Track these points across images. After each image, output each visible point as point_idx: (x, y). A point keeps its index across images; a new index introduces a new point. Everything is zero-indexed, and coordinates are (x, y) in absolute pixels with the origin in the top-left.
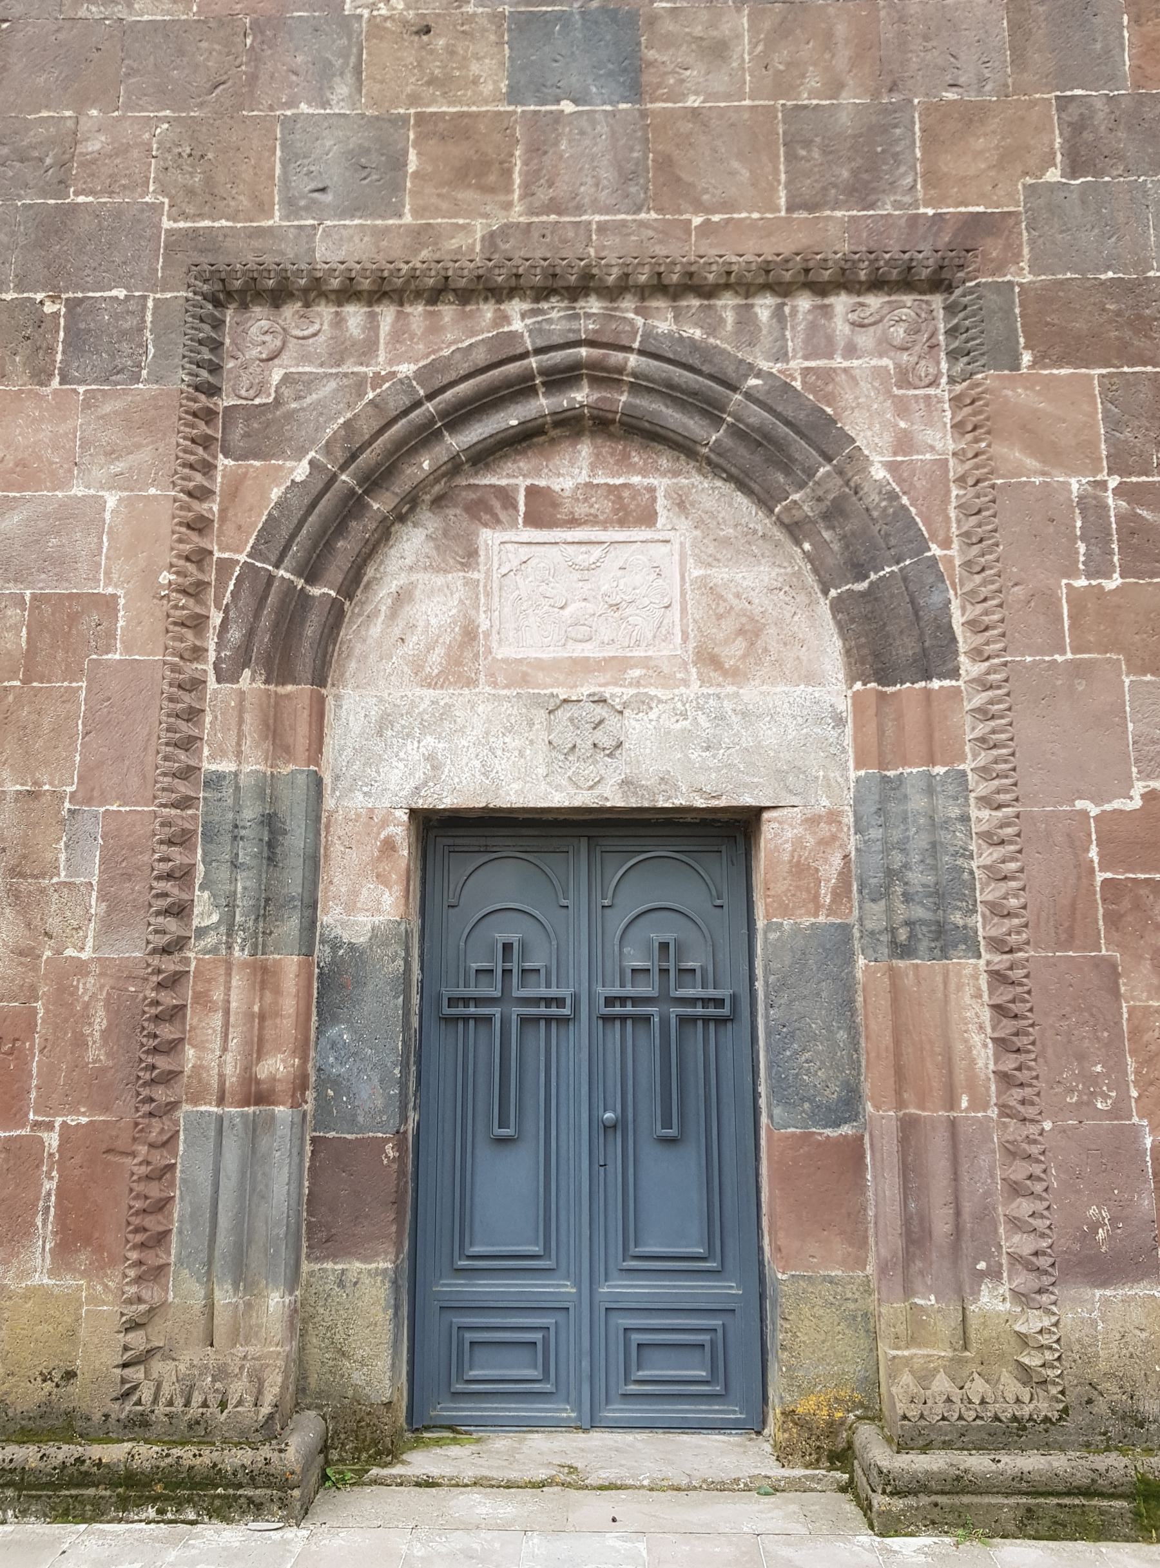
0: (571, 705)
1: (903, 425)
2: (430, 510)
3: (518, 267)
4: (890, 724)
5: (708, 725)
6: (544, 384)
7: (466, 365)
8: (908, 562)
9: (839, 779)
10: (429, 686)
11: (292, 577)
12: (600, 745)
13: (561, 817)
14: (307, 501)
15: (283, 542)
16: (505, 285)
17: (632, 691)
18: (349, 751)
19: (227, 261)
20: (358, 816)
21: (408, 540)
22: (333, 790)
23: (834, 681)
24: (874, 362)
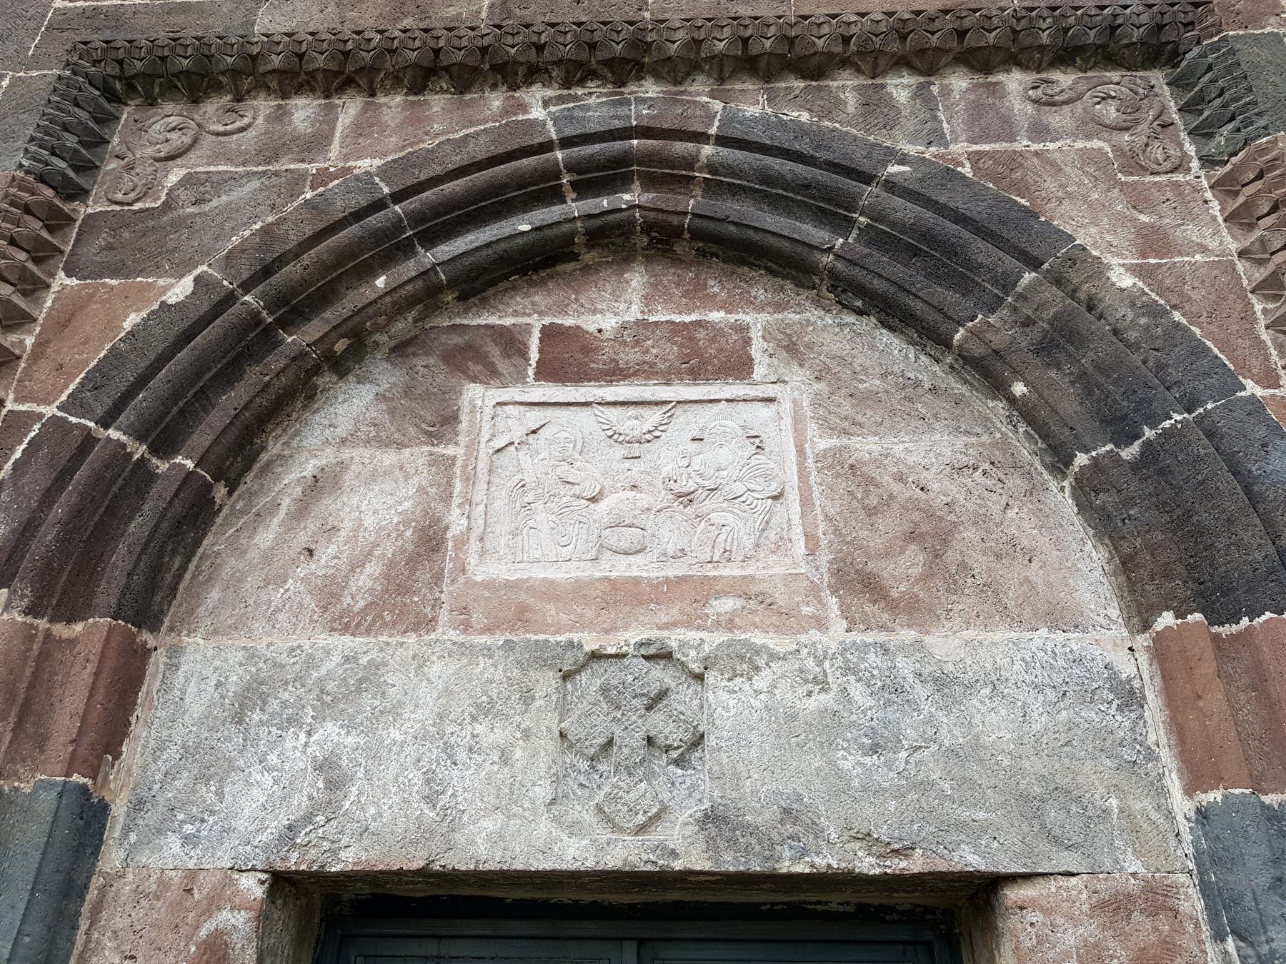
0: (605, 664)
1: (1144, 218)
2: (387, 360)
3: (540, 34)
4: (1242, 697)
5: (869, 702)
6: (574, 185)
7: (458, 158)
8: (1210, 406)
9: (1154, 815)
10: (345, 629)
11: (124, 438)
12: (661, 740)
13: (587, 898)
14: (177, 329)
15: (123, 386)
16: (522, 59)
17: (720, 637)
18: (173, 752)
19: (129, 37)
20: (164, 885)
21: (345, 400)
22: (126, 831)
23: (1104, 622)
24: (1079, 144)
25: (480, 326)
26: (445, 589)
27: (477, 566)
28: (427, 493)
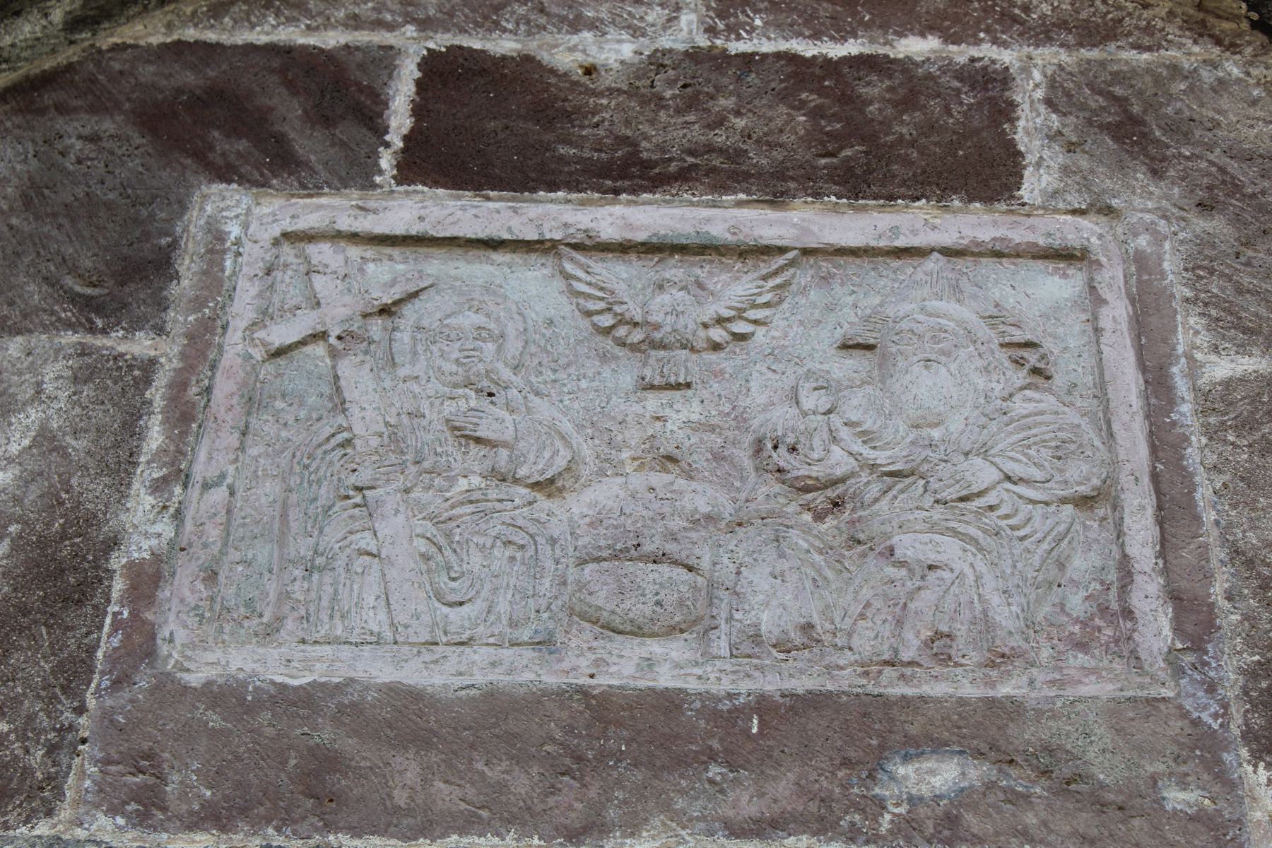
25: (251, 48)
26: (91, 702)
27: (193, 646)
28: (61, 450)
